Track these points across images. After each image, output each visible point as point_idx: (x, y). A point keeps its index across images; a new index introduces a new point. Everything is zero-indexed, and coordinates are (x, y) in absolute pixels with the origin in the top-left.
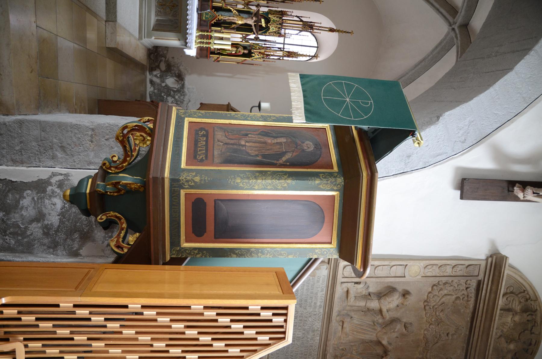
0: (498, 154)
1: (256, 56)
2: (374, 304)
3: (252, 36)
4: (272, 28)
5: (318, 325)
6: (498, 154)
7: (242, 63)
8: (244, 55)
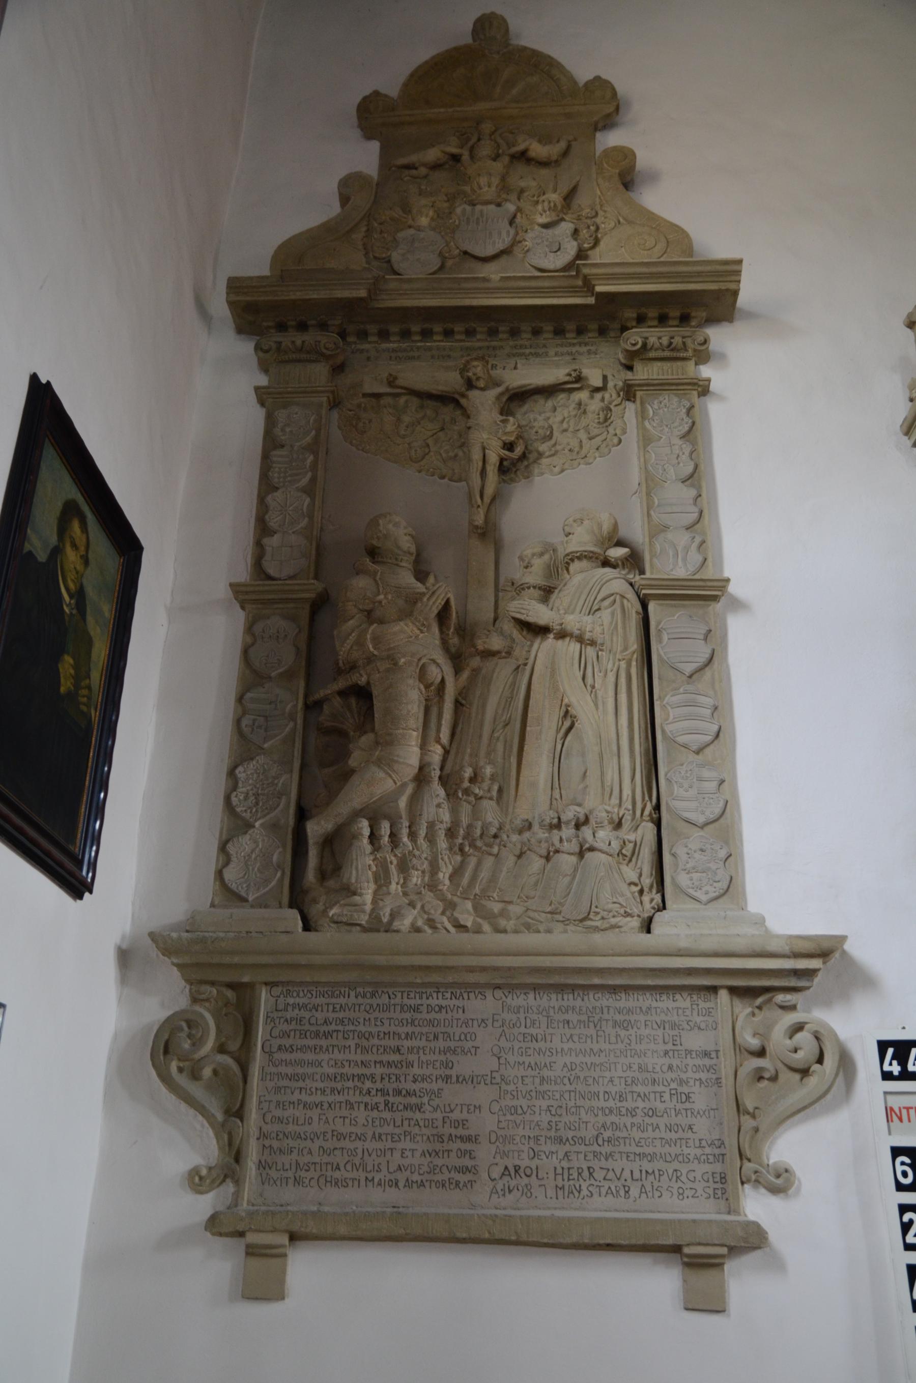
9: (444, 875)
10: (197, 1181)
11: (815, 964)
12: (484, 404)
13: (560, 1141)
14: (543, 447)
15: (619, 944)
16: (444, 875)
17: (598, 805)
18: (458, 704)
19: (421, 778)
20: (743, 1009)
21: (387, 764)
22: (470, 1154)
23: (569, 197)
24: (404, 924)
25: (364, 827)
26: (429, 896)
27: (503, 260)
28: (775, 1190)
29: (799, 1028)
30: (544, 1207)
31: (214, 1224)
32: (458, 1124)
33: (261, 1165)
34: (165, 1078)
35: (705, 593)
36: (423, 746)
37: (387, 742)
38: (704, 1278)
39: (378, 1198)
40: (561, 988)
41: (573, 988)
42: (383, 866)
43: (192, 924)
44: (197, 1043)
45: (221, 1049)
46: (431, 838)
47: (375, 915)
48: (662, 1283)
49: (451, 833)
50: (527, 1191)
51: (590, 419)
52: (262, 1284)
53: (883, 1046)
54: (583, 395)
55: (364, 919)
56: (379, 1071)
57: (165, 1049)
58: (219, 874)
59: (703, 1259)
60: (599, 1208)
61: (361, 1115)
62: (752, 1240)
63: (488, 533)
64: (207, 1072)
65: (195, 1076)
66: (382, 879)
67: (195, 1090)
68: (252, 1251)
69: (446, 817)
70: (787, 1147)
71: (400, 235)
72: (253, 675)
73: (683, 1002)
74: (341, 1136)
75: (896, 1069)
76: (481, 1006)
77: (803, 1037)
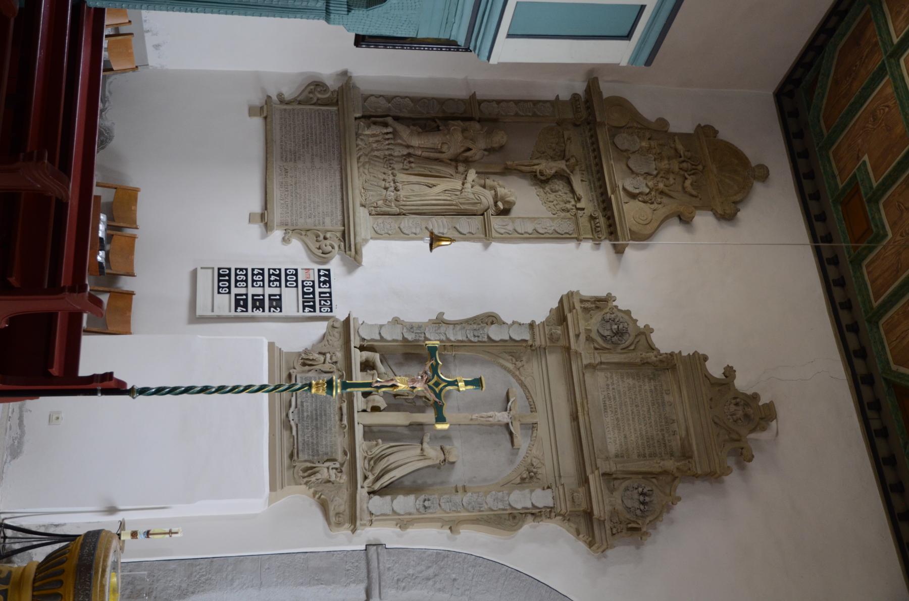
9: (376, 153)
10: (280, 95)
11: (354, 259)
12: (561, 165)
13: (296, 184)
14: (547, 189)
15: (356, 196)
16: (376, 153)
17: (402, 193)
18: (437, 160)
19: (408, 147)
20: (339, 235)
21: (412, 134)
22: (291, 160)
23: (662, 193)
24: (359, 142)
25: (390, 130)
26: (369, 149)
27: (629, 171)
28: (284, 239)
29: (333, 248)
30: (276, 180)
31: (269, 97)
32: (299, 158)
33: (285, 110)
34: (309, 85)
36: (419, 147)
37: (419, 134)
38: (259, 219)
39: (277, 135)
40: (342, 185)
41: (342, 188)
42: (377, 135)
43: (355, 87)
44: (320, 92)
45: (318, 99)
46: (388, 149)
47: (361, 135)
48: (257, 208)
49: (390, 155)
50: (280, 175)
51: (562, 205)
52: (253, 111)
53: (329, 270)
54: (573, 203)
55: (360, 132)
56: (314, 138)
57: (317, 85)
58: (372, 95)
59: (264, 219)
60: (277, 193)
61: (301, 133)
62: (268, 228)
63: (506, 171)
64: (311, 95)
65: (310, 93)
66: (373, 135)
67: (306, 93)
68: (262, 108)
69: (396, 154)
70: (296, 245)
71: (636, 137)
72: (442, 102)
73: (340, 217)
74: (294, 128)
75: (322, 273)
76: (336, 166)
77: (330, 248)
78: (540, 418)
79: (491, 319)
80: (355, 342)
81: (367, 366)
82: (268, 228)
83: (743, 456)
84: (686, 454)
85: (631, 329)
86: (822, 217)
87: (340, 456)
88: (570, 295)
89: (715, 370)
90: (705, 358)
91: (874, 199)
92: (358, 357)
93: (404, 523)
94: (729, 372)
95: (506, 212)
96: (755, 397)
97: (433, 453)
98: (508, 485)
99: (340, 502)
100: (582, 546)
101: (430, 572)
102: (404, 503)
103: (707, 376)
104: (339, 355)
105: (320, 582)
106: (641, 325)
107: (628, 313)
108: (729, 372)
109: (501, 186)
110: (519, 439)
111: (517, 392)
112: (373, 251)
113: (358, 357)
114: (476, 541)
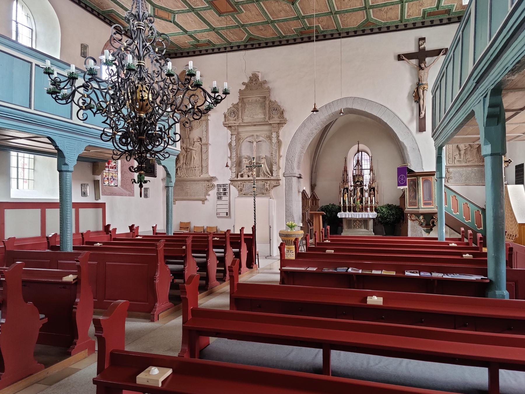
0: (411, 121)
1: (374, 185)
2: (462, 152)
3: (365, 188)
4: (361, 179)
5: (470, 169)
6: (411, 121)
7: (377, 192)
8: (374, 191)
15: (198, 178)
35: (207, 144)
39: (182, 197)
51: (198, 123)
59: (203, 201)
60: (196, 197)
62: (206, 199)
70: (210, 193)
78: (255, 134)
79: (230, 145)
80: (236, 179)
81: (242, 176)
82: (206, 199)
83: (265, 82)
84: (265, 98)
85: (233, 109)
86: (200, 51)
87: (263, 183)
88: (224, 124)
89: (243, 87)
90: (240, 90)
91: (198, 41)
92: (239, 178)
93: (279, 168)
94: (244, 84)
95: (201, 139)
96: (250, 78)
97: (263, 161)
98: (271, 143)
99: (274, 183)
100: (285, 126)
101: (290, 161)
102: (275, 168)
103: (245, 90)
104: (239, 183)
105: (292, 188)
106: (231, 106)
107: (228, 109)
108: (244, 84)
109: (194, 139)
110: (261, 139)
111: (248, 139)
112: (211, 174)
113: (239, 178)
114: (284, 151)
